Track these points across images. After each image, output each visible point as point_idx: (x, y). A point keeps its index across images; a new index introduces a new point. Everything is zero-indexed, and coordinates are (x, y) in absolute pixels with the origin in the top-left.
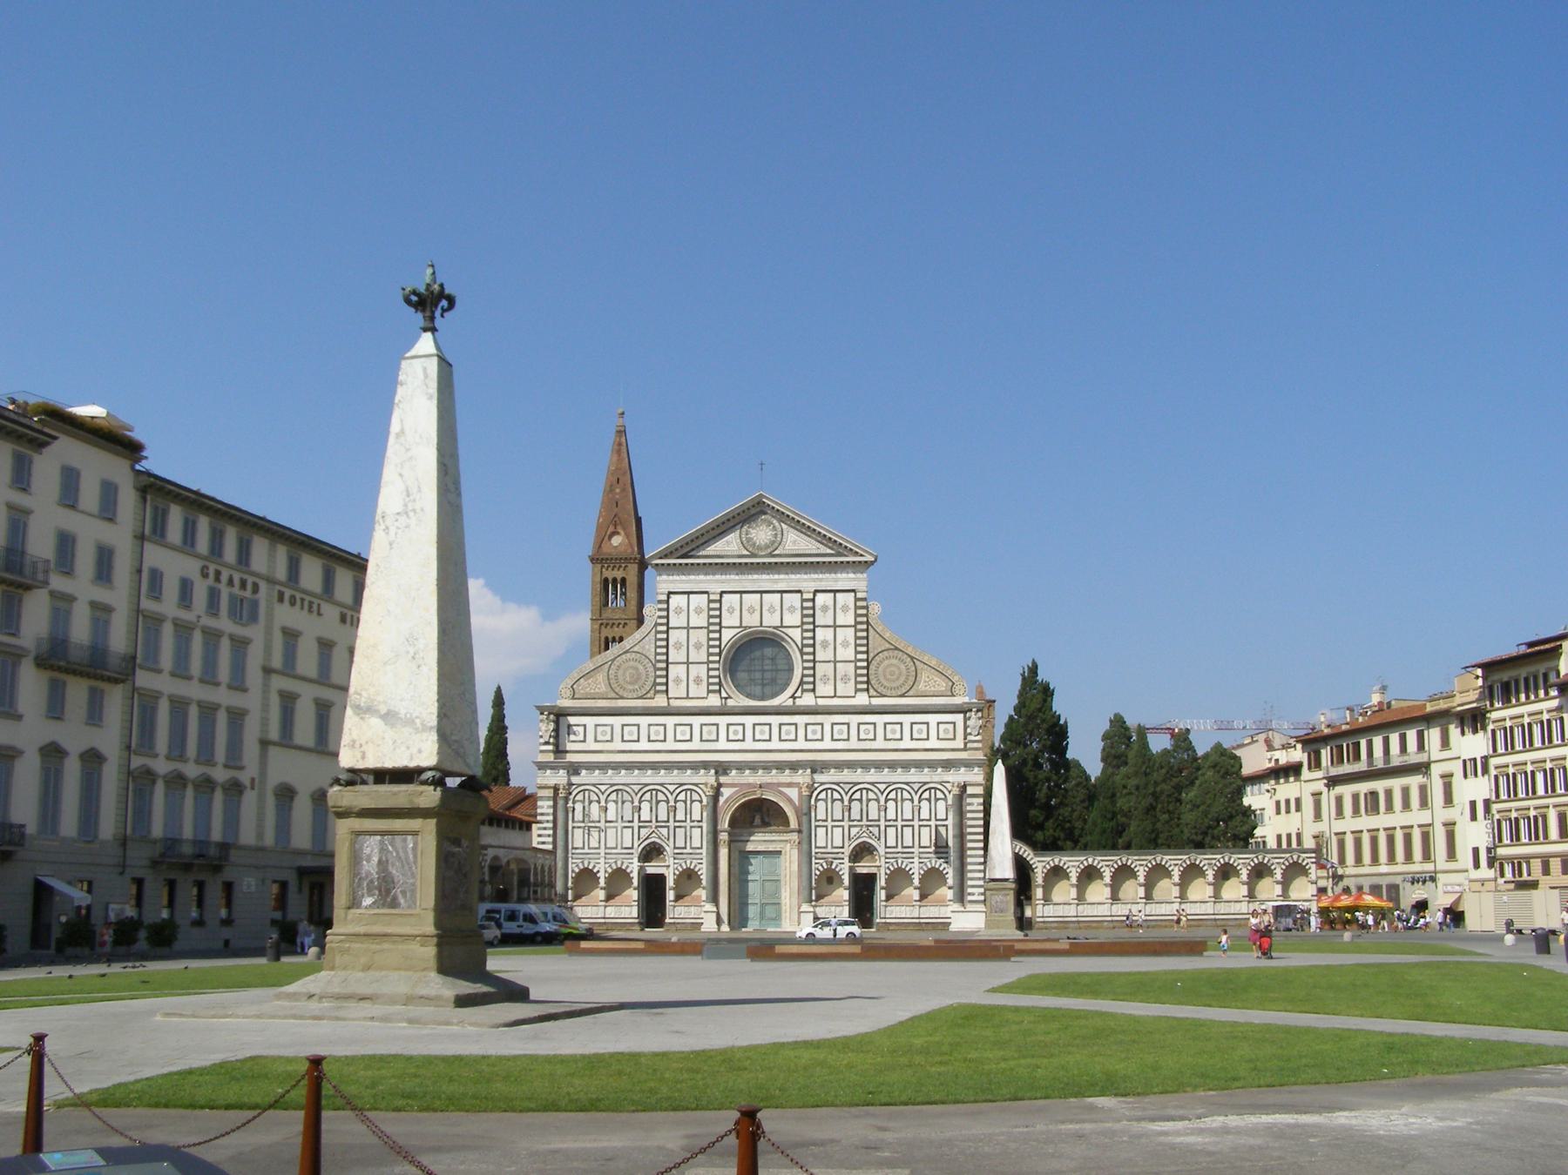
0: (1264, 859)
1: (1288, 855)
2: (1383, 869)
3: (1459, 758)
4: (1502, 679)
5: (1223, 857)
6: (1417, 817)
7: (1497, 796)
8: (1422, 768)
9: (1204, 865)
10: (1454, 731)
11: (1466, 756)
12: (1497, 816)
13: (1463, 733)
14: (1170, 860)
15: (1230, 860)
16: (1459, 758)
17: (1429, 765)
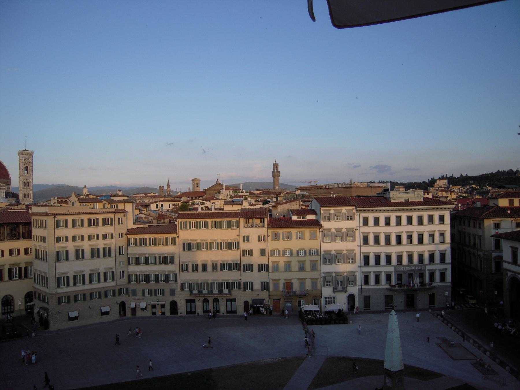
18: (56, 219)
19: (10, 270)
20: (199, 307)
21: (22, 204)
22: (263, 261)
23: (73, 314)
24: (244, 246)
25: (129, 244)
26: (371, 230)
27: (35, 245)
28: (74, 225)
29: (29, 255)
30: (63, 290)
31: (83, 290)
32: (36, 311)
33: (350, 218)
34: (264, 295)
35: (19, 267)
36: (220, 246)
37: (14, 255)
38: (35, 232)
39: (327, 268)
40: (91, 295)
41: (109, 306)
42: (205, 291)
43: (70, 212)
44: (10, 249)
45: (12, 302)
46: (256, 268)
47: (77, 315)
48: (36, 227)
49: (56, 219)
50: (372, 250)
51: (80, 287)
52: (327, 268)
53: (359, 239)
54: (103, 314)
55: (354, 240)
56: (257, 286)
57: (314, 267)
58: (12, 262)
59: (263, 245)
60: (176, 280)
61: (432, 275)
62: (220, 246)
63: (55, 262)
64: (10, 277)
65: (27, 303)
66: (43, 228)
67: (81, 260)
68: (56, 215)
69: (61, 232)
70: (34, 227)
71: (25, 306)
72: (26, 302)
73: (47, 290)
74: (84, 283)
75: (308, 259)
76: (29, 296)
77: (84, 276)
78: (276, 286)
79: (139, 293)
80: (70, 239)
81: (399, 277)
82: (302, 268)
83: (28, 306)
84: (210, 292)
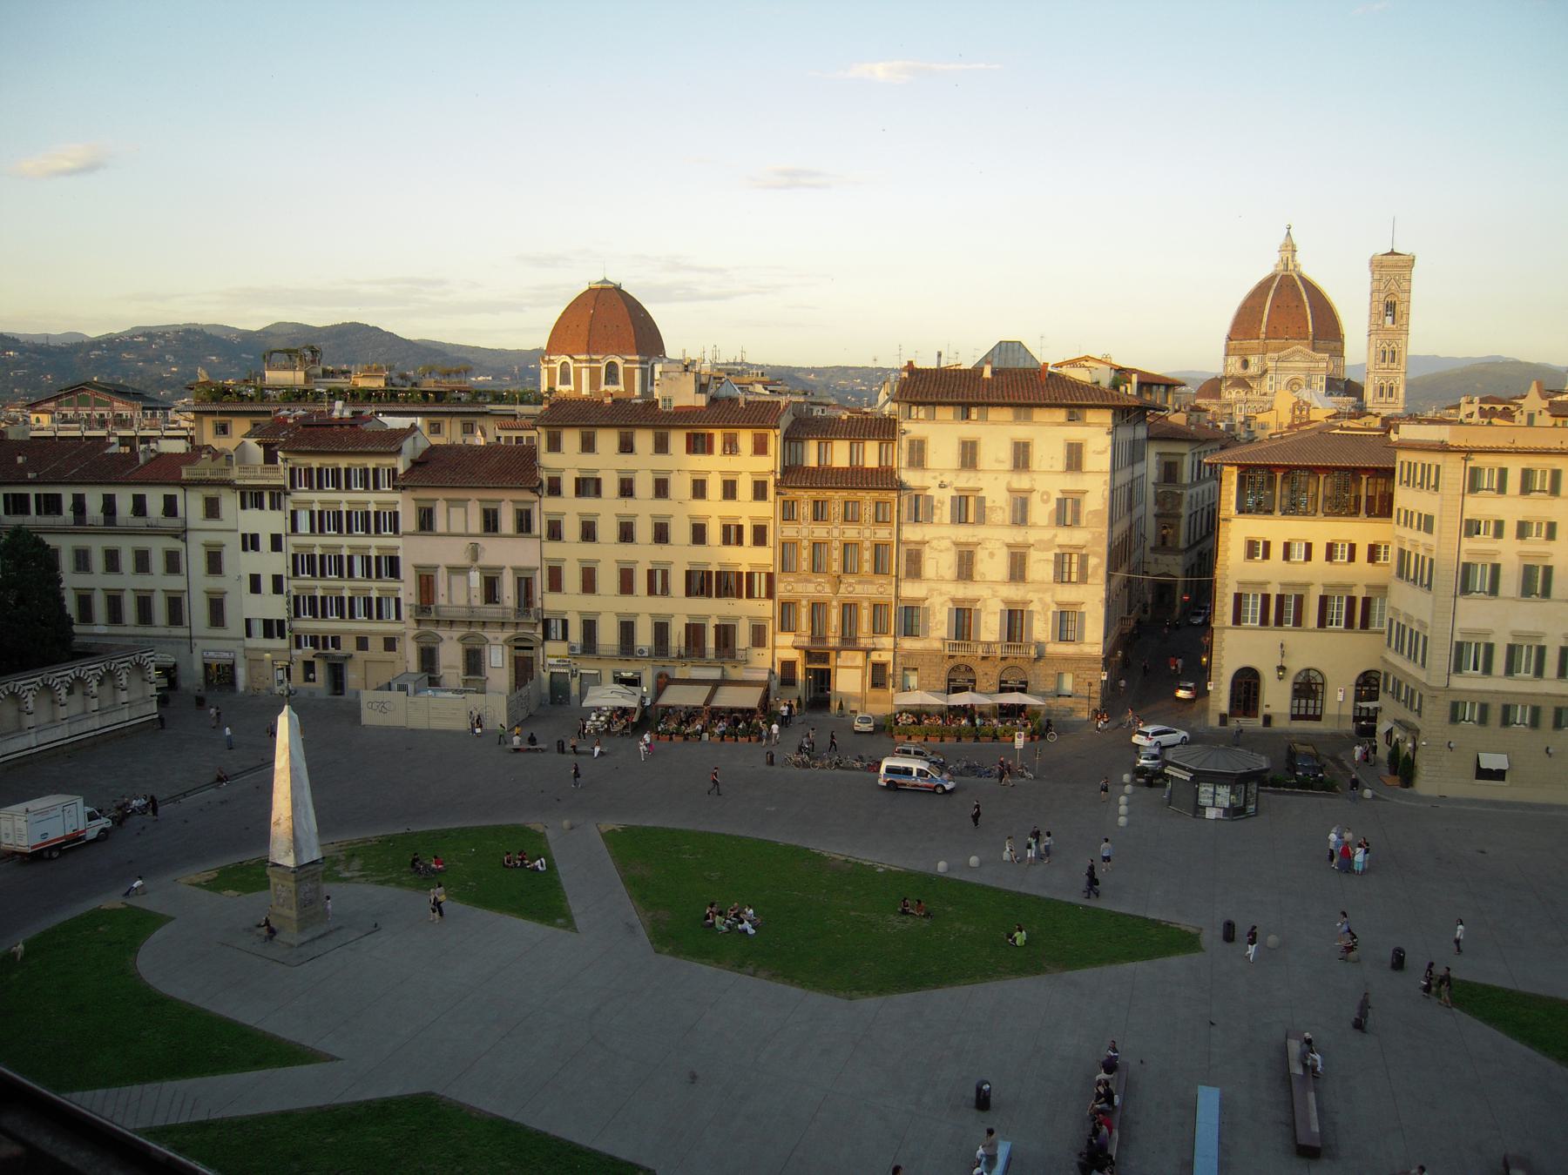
0: (111, 666)
1: (132, 658)
2: (101, 629)
3: (237, 531)
4: (338, 464)
5: (74, 672)
6: (159, 581)
7: (295, 573)
8: (181, 534)
9: (57, 684)
10: (229, 502)
11: (242, 530)
12: (294, 592)
13: (243, 507)
14: (24, 685)
15: (80, 673)
16: (237, 531)
17: (185, 531)
18: (1470, 464)
19: (1324, 601)
21: (1371, 414)
23: (1490, 761)
27: (1401, 539)
28: (1526, 488)
29: (1381, 565)
30: (1470, 682)
31: (1533, 694)
32: (1382, 727)
35: (1264, 593)
37: (1339, 560)
38: (1404, 498)
40: (1507, 711)
41: (1506, 756)
43: (1519, 444)
44: (1329, 542)
45: (1320, 690)
47: (1505, 766)
48: (1408, 485)
49: (1470, 464)
51: (1523, 684)
54: (1484, 774)
58: (1333, 580)
63: (1455, 596)
64: (1322, 622)
65: (1362, 701)
66: (1428, 488)
67: (1538, 599)
68: (1472, 452)
69: (1483, 507)
70: (1401, 484)
71: (1355, 709)
72: (1358, 698)
73: (1422, 676)
74: (1539, 672)
76: (1368, 684)
77: (1541, 651)
80: (1510, 529)
83: (1361, 708)
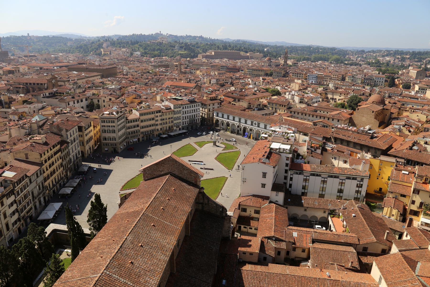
20: (145, 138)
22: (161, 122)
24: (156, 119)
25: (126, 123)
26: (184, 110)
33: (180, 107)
34: (161, 132)
36: (150, 120)
39: (175, 122)
42: (147, 133)
46: (159, 125)
50: (184, 115)
52: (175, 122)
53: (182, 113)
55: (181, 113)
56: (159, 130)
57: (172, 122)
59: (161, 118)
60: (139, 132)
61: (196, 120)
62: (150, 120)
75: (171, 120)
78: (164, 129)
79: (130, 138)
81: (190, 121)
82: (169, 123)
84: (148, 133)
